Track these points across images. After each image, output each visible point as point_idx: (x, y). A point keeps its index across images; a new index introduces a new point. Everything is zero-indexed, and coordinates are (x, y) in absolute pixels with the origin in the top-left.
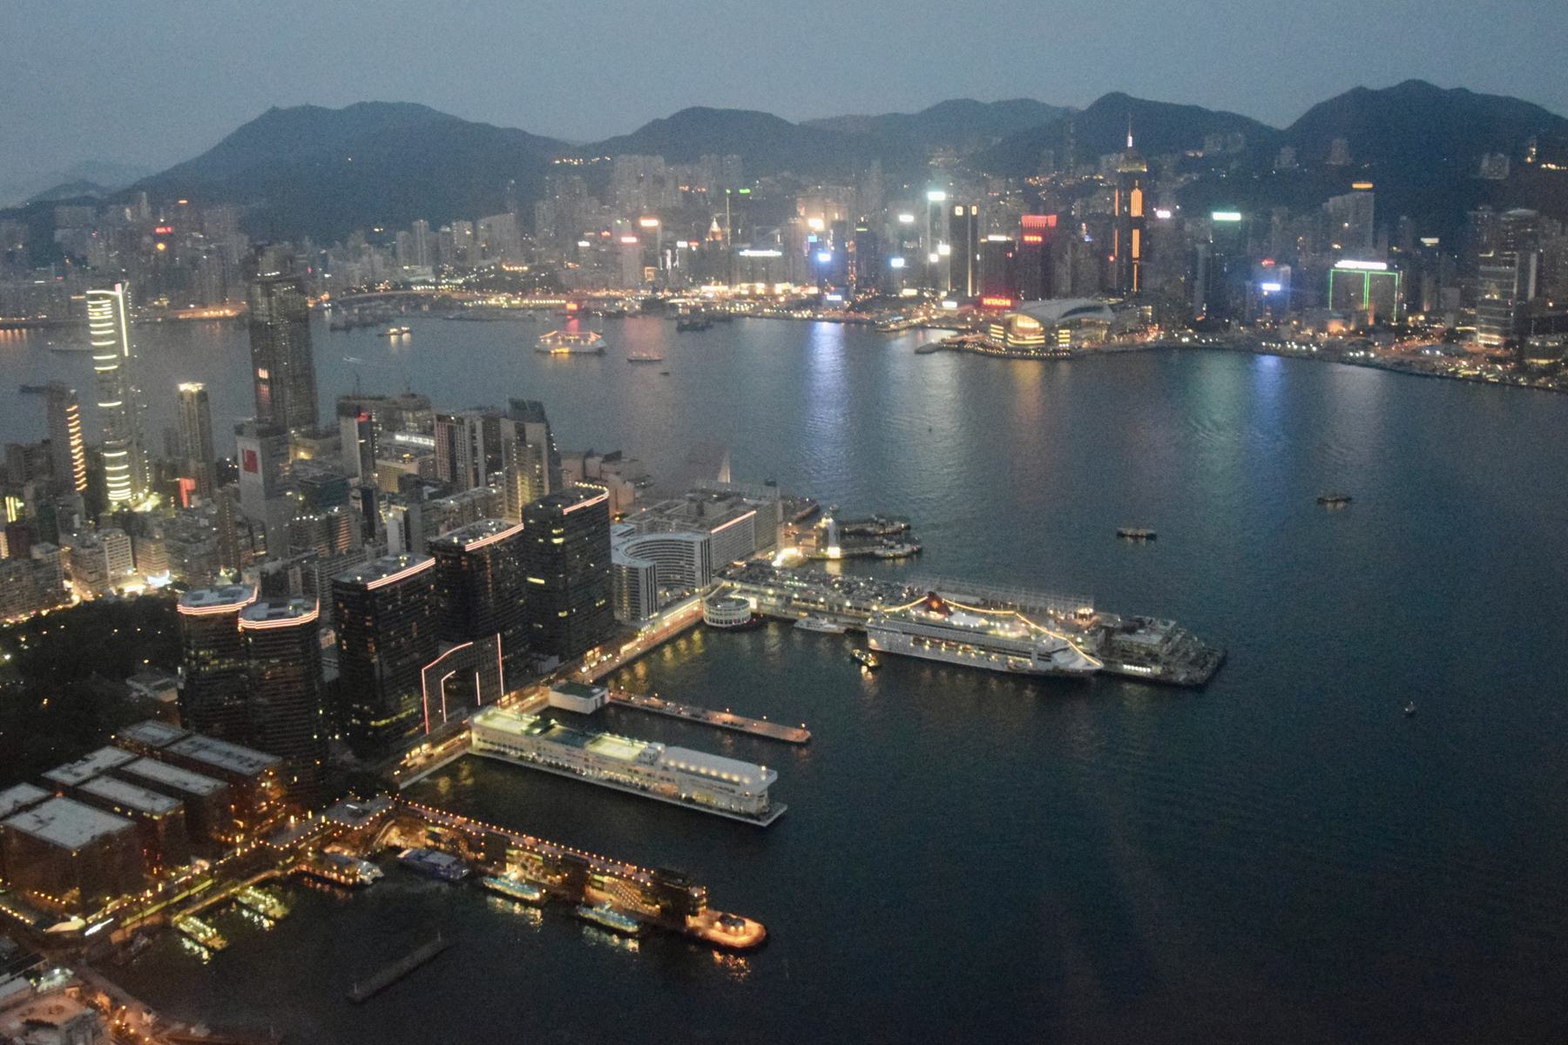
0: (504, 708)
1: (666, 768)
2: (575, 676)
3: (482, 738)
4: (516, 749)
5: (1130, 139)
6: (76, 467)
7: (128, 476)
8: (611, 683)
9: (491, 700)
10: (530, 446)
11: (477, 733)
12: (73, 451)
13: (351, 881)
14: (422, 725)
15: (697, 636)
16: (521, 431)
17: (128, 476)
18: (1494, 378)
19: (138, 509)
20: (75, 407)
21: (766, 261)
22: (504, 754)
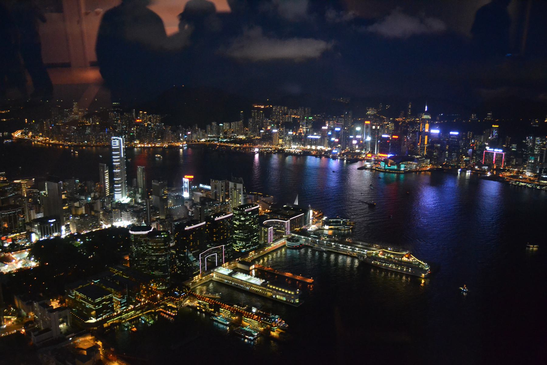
0: (224, 267)
1: (269, 288)
2: (246, 259)
3: (216, 276)
4: (226, 279)
5: (426, 107)
6: (107, 188)
7: (121, 192)
8: (257, 262)
9: (220, 264)
10: (238, 190)
11: (215, 274)
12: (106, 184)
13: (174, 314)
14: (199, 271)
15: (283, 250)
16: (235, 186)
17: (121, 192)
18: (531, 186)
19: (123, 202)
20: (107, 171)
21: (316, 139)
22: (223, 281)
